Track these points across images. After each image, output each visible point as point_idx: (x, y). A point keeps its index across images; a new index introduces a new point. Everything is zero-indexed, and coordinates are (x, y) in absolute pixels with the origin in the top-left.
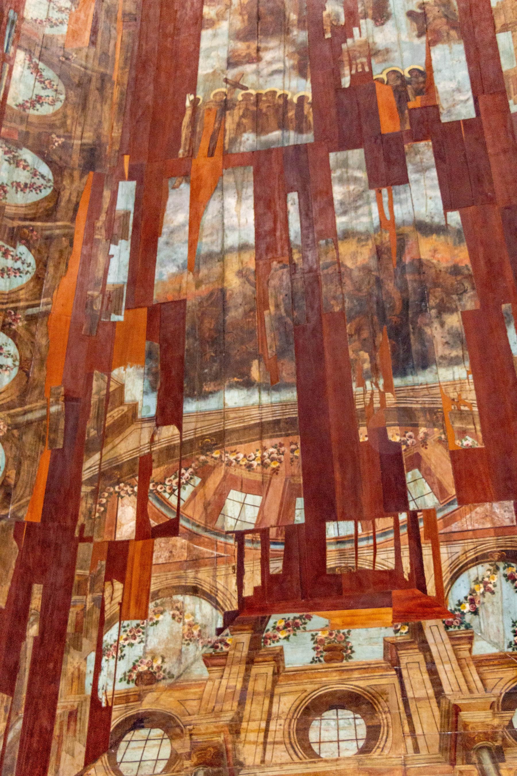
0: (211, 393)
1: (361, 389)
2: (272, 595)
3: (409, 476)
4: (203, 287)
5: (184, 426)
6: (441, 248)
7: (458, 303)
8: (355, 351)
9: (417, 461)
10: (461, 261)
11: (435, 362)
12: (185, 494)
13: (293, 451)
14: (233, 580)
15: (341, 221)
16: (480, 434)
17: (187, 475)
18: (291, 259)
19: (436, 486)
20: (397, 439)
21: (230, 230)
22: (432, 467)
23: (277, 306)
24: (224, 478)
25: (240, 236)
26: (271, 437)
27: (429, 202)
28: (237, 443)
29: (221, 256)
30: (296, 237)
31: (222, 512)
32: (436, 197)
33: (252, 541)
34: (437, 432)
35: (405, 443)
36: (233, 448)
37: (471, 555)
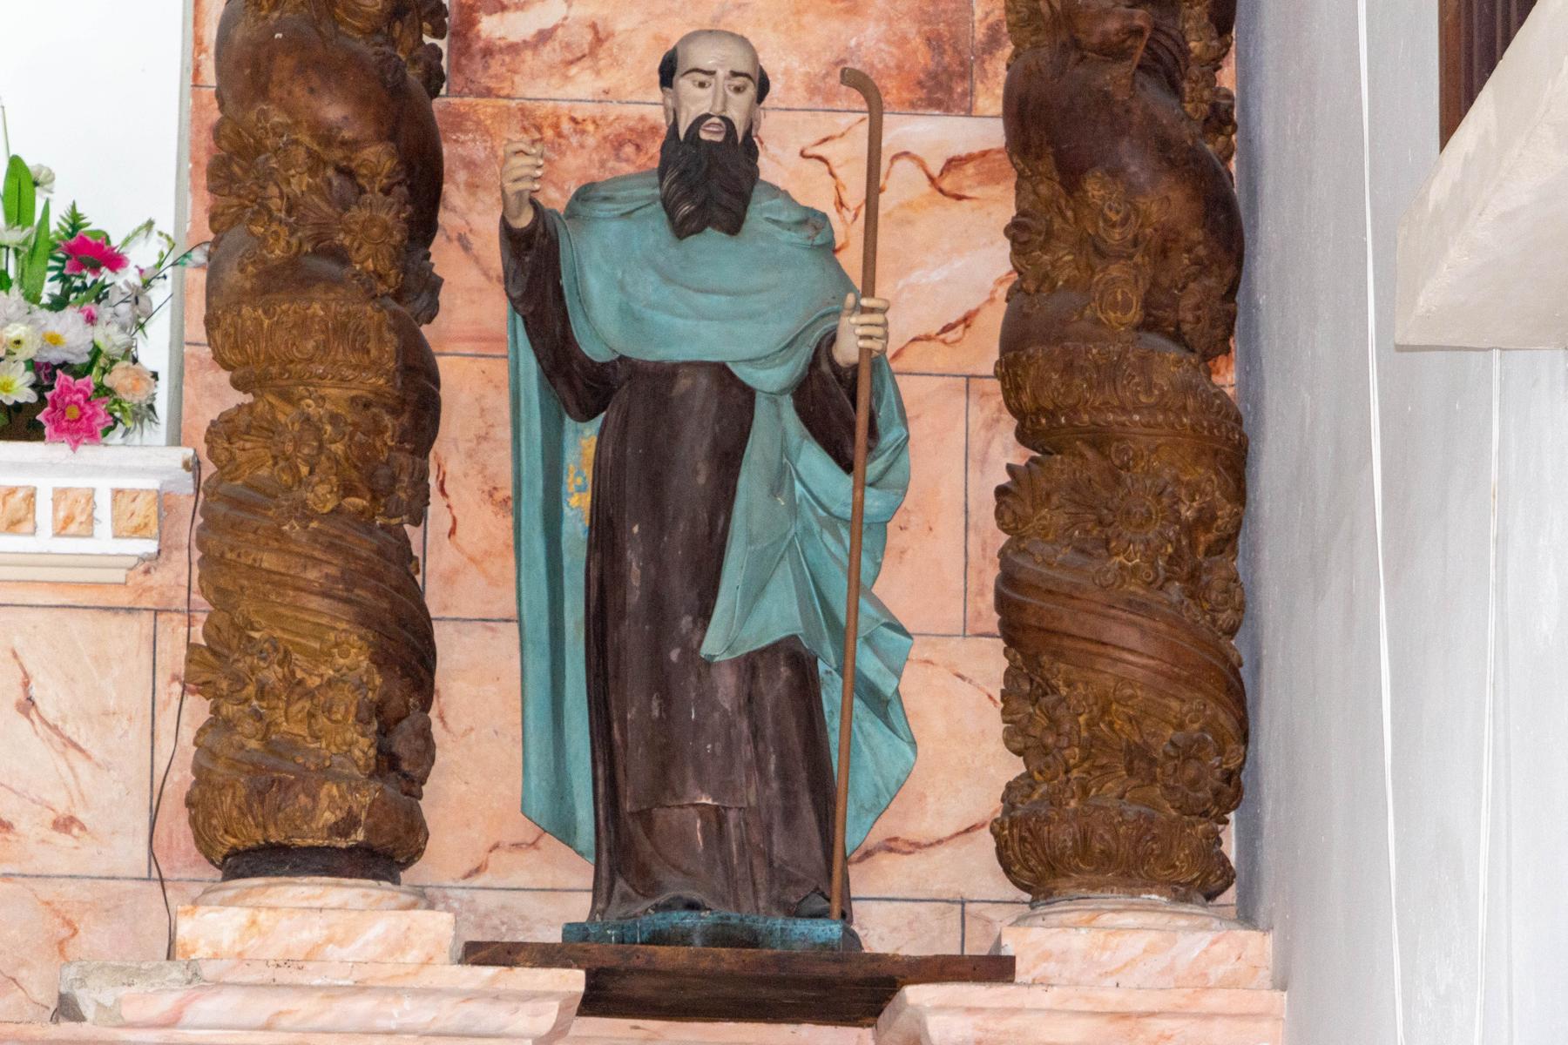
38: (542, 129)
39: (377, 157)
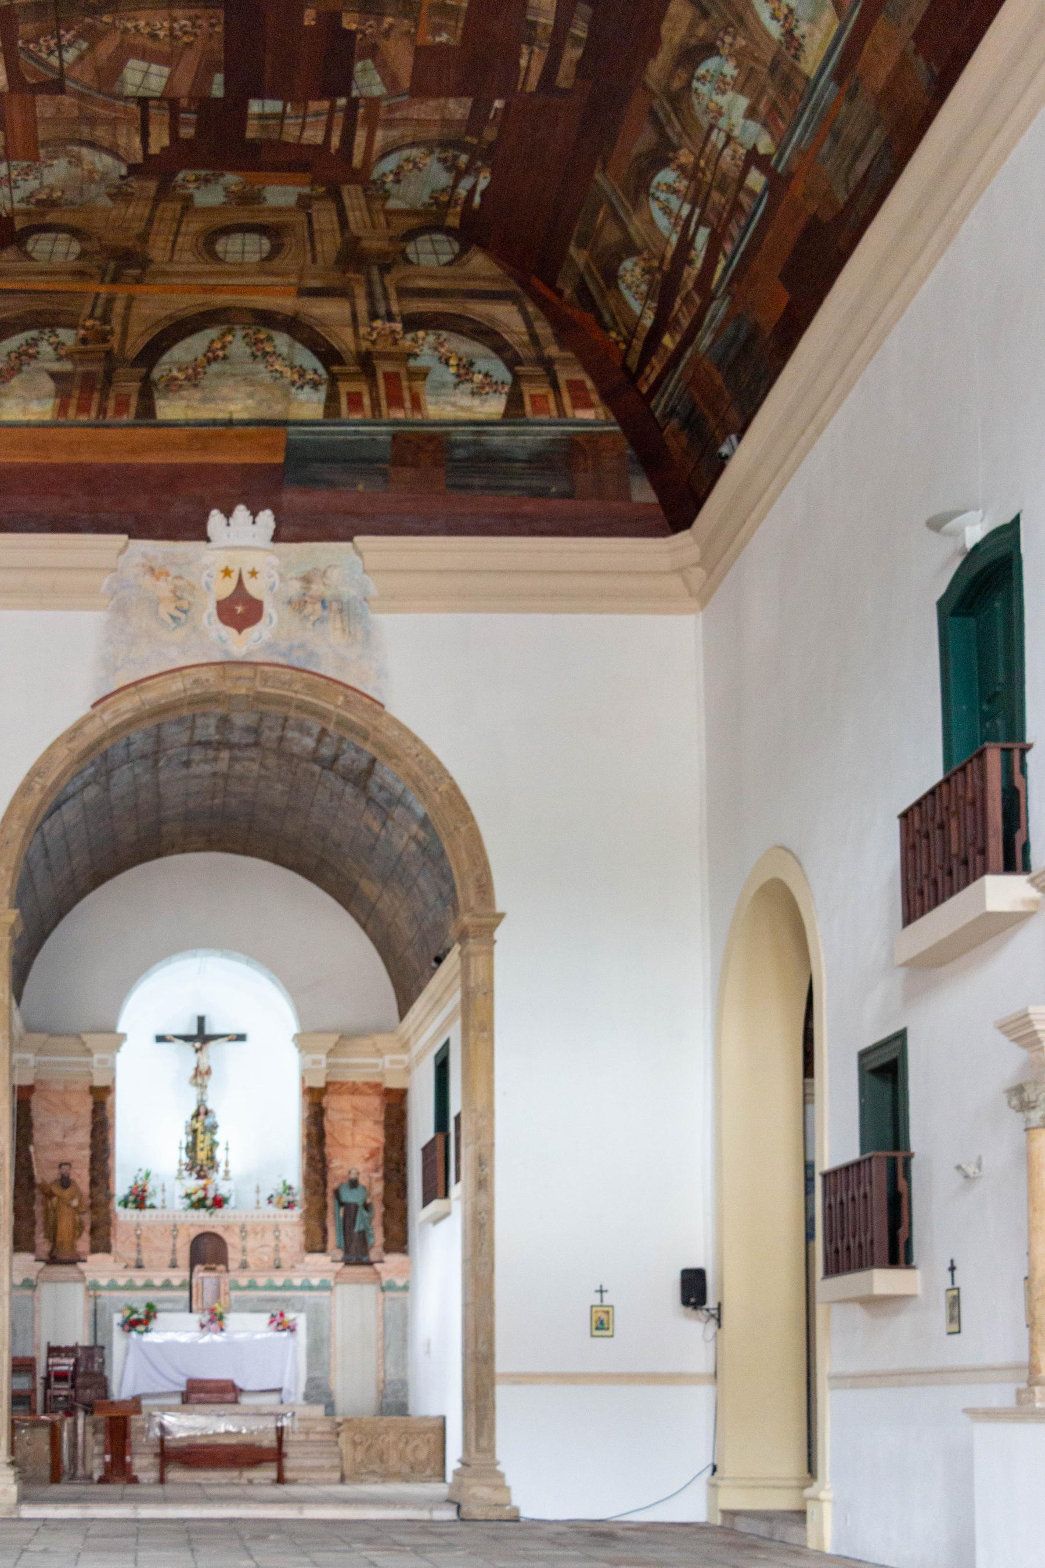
2: (182, 154)
3: (359, 66)
9: (373, 51)
12: (70, 56)
14: (137, 141)
16: (459, 32)
17: (68, 37)
20: (354, 27)
22: (390, 60)
24: (121, 46)
26: (184, 7)
28: (135, 10)
31: (120, 78)
33: (159, 108)
34: (406, 24)
36: (132, 14)
37: (409, 140)
38: (336, 1178)
39: (321, 1182)
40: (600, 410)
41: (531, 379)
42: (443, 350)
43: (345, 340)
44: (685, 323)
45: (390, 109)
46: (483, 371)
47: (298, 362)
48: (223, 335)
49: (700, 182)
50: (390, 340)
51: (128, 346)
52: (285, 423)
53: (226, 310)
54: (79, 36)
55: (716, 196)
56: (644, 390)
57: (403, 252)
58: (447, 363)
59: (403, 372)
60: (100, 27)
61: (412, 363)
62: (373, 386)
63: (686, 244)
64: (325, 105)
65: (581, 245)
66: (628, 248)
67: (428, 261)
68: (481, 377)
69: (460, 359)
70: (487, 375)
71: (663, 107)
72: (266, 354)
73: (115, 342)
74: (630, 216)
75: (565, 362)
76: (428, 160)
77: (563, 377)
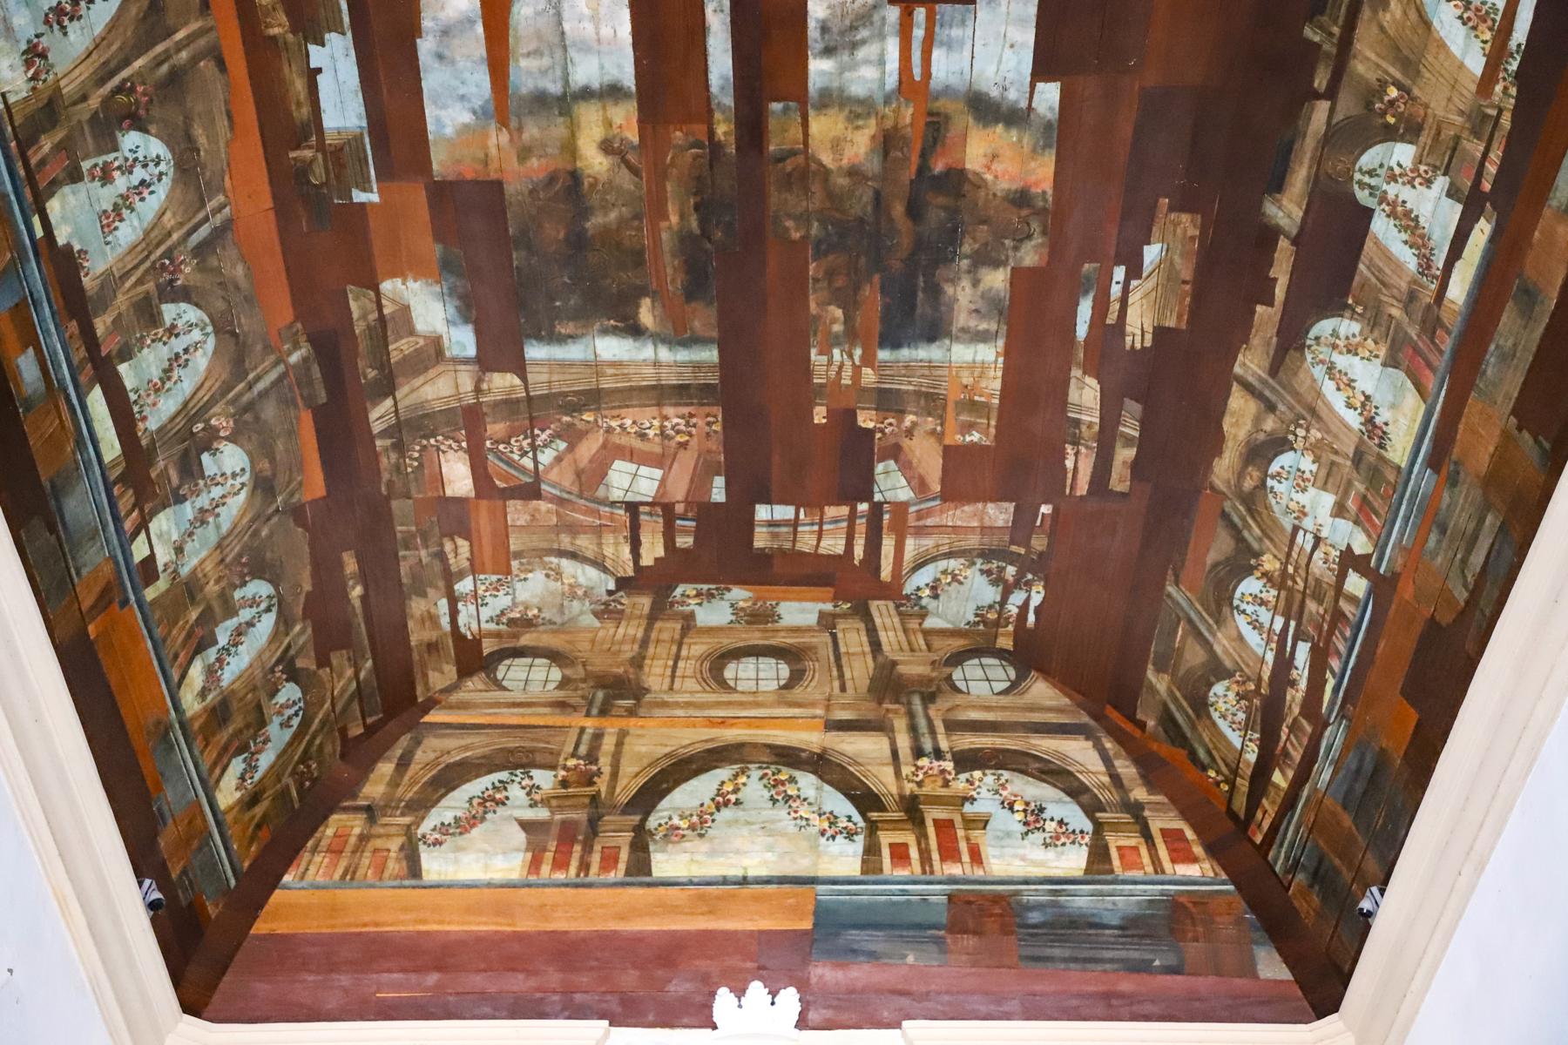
0: (571, 337)
1: (824, 359)
3: (880, 468)
4: (534, 162)
5: (529, 376)
6: (1007, 153)
7: (1010, 253)
8: (822, 304)
10: (1037, 184)
11: (949, 335)
12: (546, 457)
13: (709, 424)
14: (626, 551)
15: (819, 69)
16: (993, 431)
17: (544, 436)
18: (711, 133)
19: (915, 482)
20: (871, 425)
21: (580, 50)
22: (915, 461)
23: (682, 216)
24: (604, 446)
25: (602, 67)
26: (676, 405)
27: (1008, 52)
28: (620, 407)
29: (566, 102)
30: (723, 88)
32: (1023, 45)
33: (650, 514)
35: (882, 431)
36: (615, 412)
37: (945, 549)
40: (1207, 865)
41: (1116, 827)
42: (1005, 793)
43: (884, 781)
44: (1297, 755)
45: (920, 515)
46: (1057, 818)
47: (827, 808)
48: (736, 776)
49: (1291, 591)
50: (940, 782)
51: (618, 790)
52: (813, 881)
53: (740, 746)
54: (557, 435)
55: (1311, 606)
56: (1258, 839)
57: (949, 678)
58: (1011, 808)
59: (958, 819)
60: (580, 425)
61: (968, 808)
62: (922, 836)
63: (1284, 663)
64: (844, 510)
65: (1160, 669)
66: (1216, 670)
67: (979, 689)
68: (1054, 824)
69: (1027, 804)
70: (1061, 822)
71: (1237, 510)
72: (788, 798)
73: (602, 785)
74: (1214, 635)
75: (1157, 807)
76: (969, 572)
77: (1156, 826)
